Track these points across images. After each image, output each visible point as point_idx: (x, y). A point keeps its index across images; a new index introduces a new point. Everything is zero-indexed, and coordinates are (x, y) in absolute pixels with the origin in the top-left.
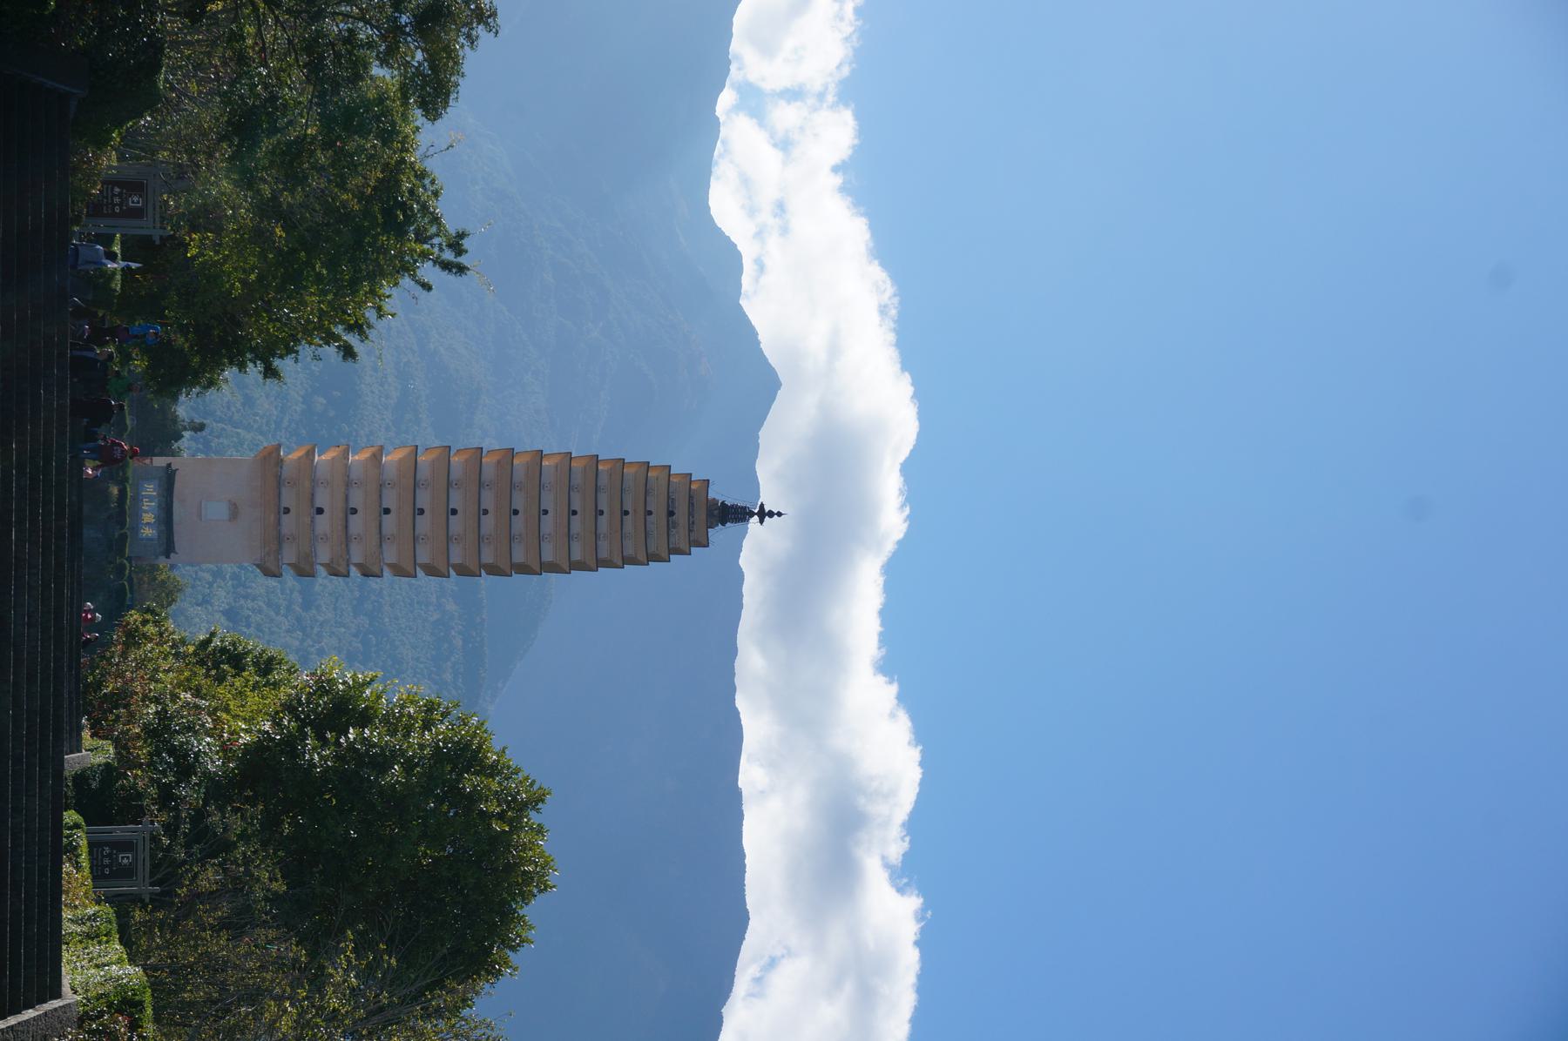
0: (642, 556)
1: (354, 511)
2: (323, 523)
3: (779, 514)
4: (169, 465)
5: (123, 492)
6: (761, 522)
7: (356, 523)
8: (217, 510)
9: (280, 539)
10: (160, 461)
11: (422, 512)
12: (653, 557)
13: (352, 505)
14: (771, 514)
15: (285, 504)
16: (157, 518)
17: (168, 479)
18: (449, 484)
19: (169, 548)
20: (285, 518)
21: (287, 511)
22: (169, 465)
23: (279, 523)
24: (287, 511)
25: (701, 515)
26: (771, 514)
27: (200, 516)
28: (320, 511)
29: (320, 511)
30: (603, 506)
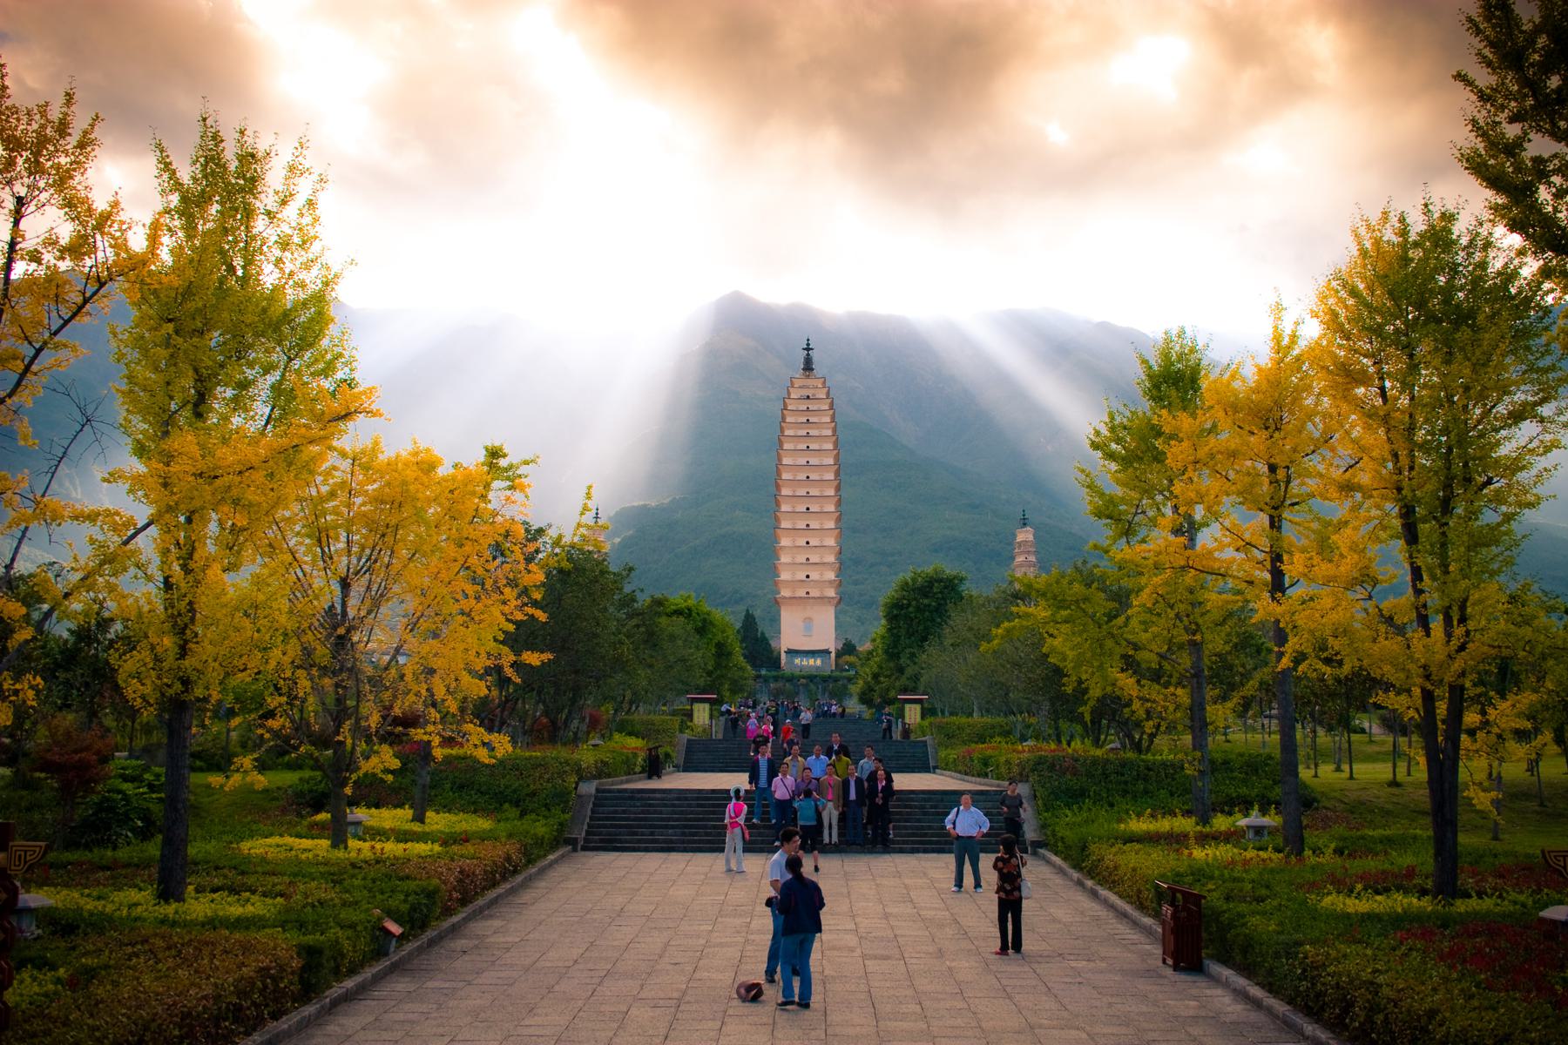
10: (783, 656)
19: (827, 652)
25: (809, 382)
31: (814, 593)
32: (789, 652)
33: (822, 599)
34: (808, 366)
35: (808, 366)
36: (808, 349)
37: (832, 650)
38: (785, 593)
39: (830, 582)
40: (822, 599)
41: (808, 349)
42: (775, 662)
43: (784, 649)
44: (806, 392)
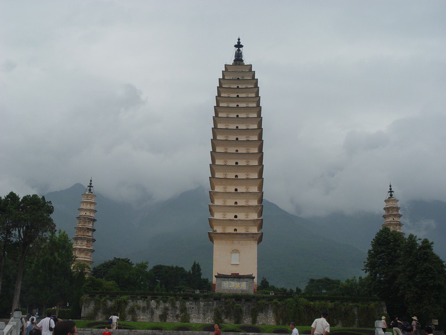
0: (256, 90)
3: (239, 39)
4: (216, 276)
6: (242, 46)
10: (214, 279)
11: (236, 176)
12: (256, 86)
13: (233, 204)
14: (239, 43)
19: (251, 277)
22: (216, 276)
25: (239, 68)
26: (239, 43)
28: (236, 217)
29: (236, 217)
30: (234, 105)
31: (241, 230)
32: (219, 276)
33: (247, 236)
34: (239, 58)
35: (239, 58)
36: (239, 46)
37: (255, 275)
38: (219, 230)
39: (254, 221)
40: (247, 236)
41: (239, 46)
42: (206, 286)
43: (215, 274)
44: (235, 77)
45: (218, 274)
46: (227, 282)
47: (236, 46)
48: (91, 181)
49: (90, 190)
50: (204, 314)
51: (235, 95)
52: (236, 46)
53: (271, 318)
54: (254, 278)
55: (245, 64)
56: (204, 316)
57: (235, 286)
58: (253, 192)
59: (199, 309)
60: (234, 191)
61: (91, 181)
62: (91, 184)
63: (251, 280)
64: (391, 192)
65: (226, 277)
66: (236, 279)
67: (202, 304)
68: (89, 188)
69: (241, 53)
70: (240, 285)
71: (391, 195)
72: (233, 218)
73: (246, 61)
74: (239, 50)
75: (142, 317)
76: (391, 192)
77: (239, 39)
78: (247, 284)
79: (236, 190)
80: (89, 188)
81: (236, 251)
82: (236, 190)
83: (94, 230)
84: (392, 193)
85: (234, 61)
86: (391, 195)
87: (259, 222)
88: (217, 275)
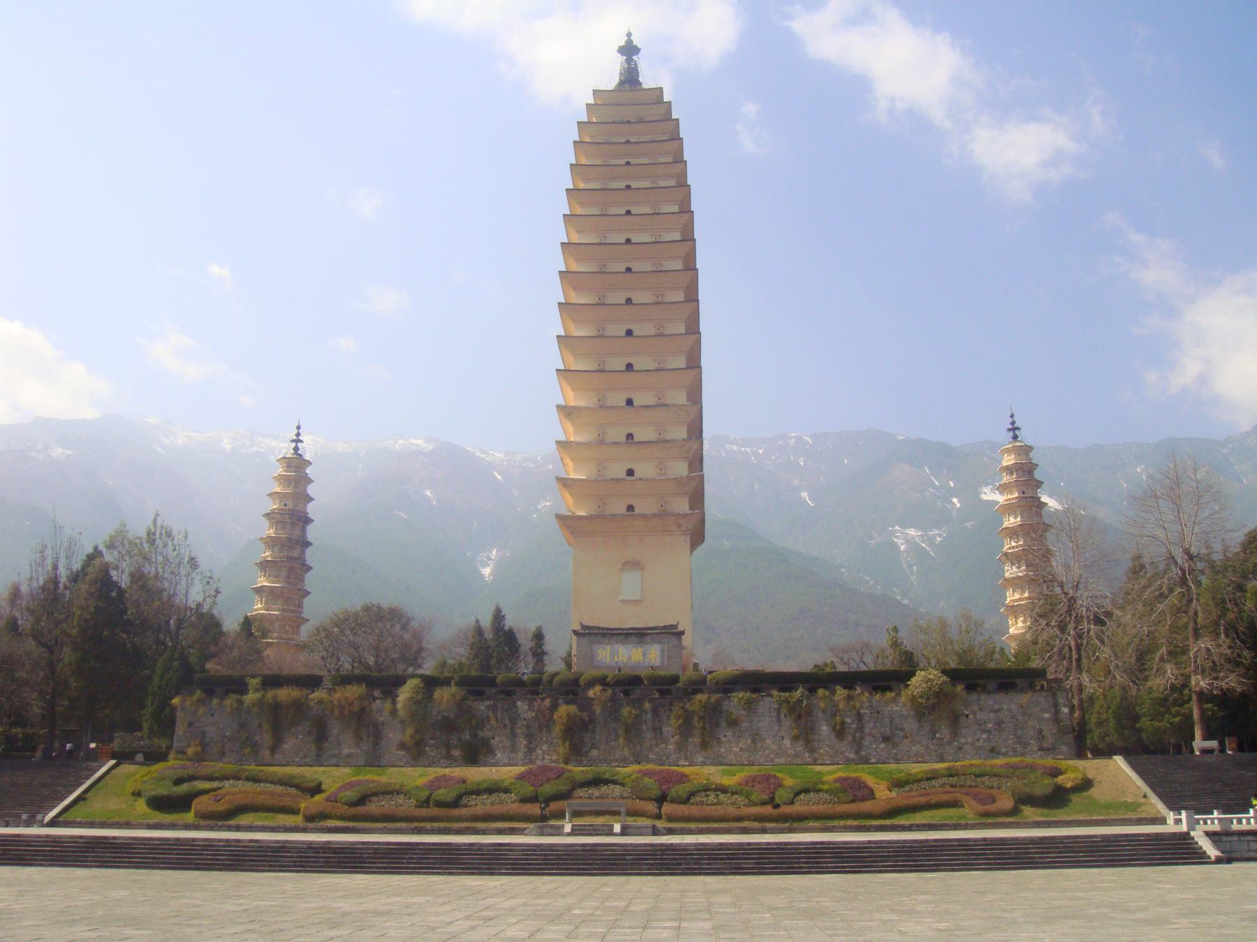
0: (672, 146)
1: (630, 436)
2: (645, 469)
3: (629, 35)
5: (602, 681)
7: (644, 433)
8: (630, 584)
9: (662, 515)
12: (676, 138)
13: (623, 439)
14: (629, 42)
15: (623, 511)
16: (641, 643)
17: (591, 634)
18: (602, 336)
19: (672, 633)
20: (638, 511)
21: (630, 508)
23: (644, 516)
24: (630, 508)
26: (629, 42)
27: (637, 602)
28: (630, 472)
29: (630, 472)
30: (622, 185)
35: (630, 78)
39: (679, 481)
45: (584, 627)
46: (608, 648)
47: (622, 50)
48: (298, 428)
49: (296, 449)
50: (530, 737)
51: (623, 162)
52: (622, 50)
53: (729, 742)
54: (683, 633)
55: (645, 86)
56: (530, 742)
57: (630, 658)
58: (675, 405)
59: (514, 721)
60: (624, 404)
61: (298, 428)
62: (298, 435)
63: (674, 639)
64: (1014, 429)
65: (604, 635)
66: (633, 638)
67: (522, 705)
68: (293, 445)
69: (636, 65)
70: (644, 655)
71: (1015, 438)
72: (623, 475)
73: (648, 80)
74: (629, 60)
75: (346, 751)
76: (1014, 429)
77: (629, 35)
78: (663, 651)
79: (629, 402)
80: (293, 445)
81: (634, 565)
82: (629, 402)
83: (307, 544)
84: (1017, 432)
85: (621, 83)
86: (1015, 438)
87: (693, 483)
88: (578, 627)
